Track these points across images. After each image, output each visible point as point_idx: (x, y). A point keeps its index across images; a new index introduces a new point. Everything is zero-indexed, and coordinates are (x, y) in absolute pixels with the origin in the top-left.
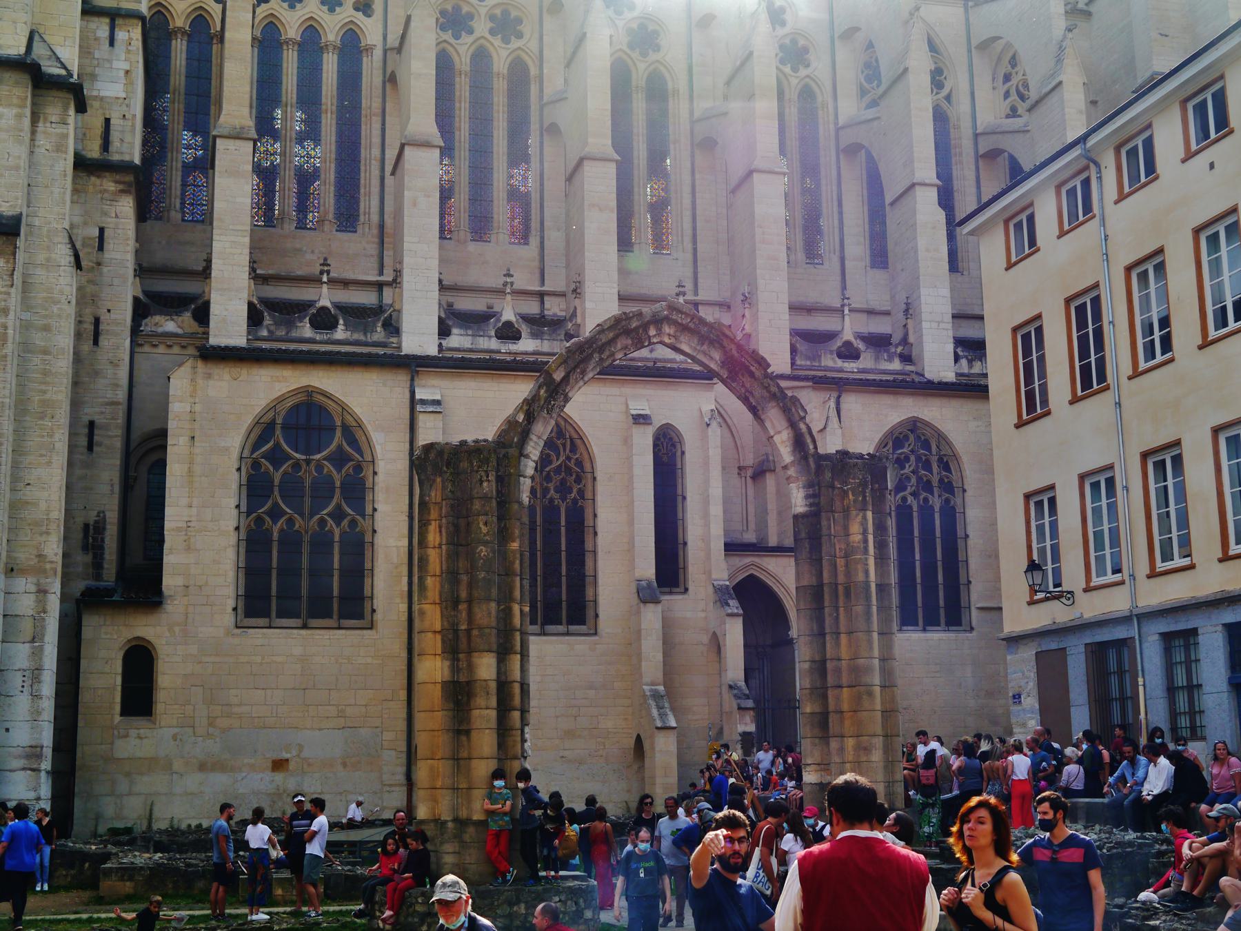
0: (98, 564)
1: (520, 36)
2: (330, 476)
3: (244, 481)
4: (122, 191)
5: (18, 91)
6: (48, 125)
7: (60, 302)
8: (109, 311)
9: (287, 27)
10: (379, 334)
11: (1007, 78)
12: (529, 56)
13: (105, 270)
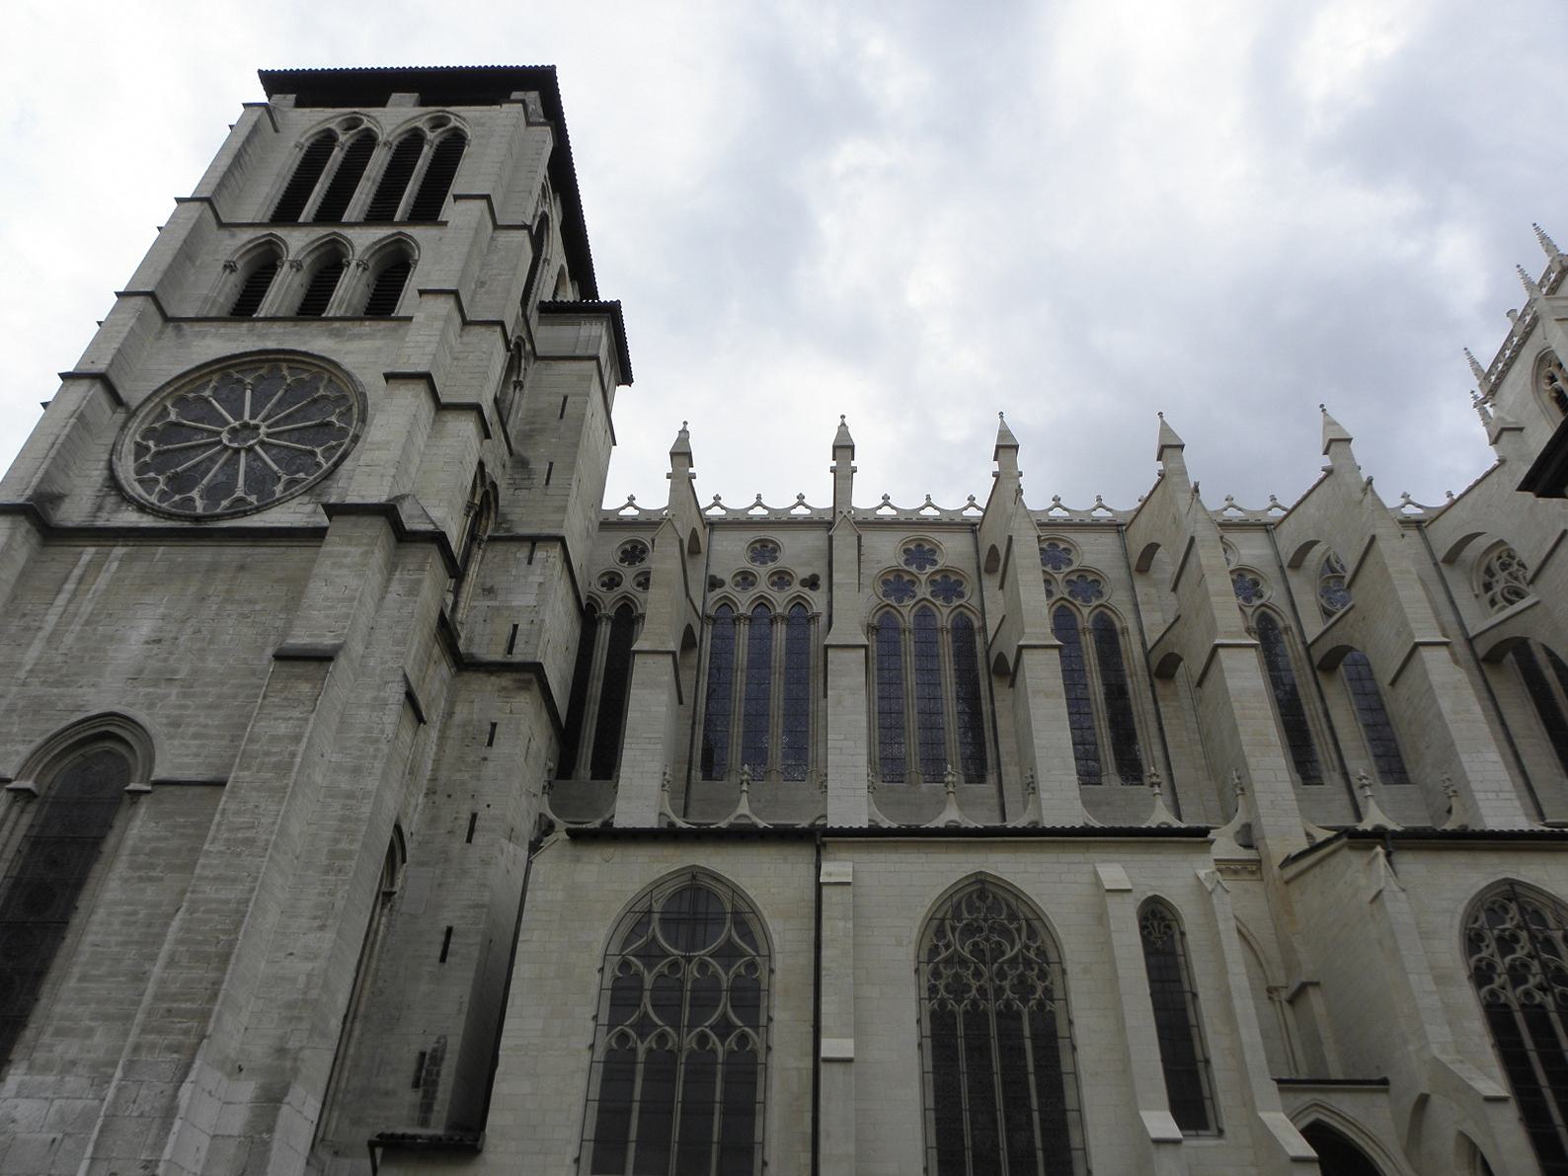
0: (427, 1107)
1: (961, 595)
2: (715, 977)
3: (608, 983)
4: (520, 688)
8: (488, 806)
9: (739, 604)
11: (1488, 587)
12: (973, 612)
13: (491, 764)
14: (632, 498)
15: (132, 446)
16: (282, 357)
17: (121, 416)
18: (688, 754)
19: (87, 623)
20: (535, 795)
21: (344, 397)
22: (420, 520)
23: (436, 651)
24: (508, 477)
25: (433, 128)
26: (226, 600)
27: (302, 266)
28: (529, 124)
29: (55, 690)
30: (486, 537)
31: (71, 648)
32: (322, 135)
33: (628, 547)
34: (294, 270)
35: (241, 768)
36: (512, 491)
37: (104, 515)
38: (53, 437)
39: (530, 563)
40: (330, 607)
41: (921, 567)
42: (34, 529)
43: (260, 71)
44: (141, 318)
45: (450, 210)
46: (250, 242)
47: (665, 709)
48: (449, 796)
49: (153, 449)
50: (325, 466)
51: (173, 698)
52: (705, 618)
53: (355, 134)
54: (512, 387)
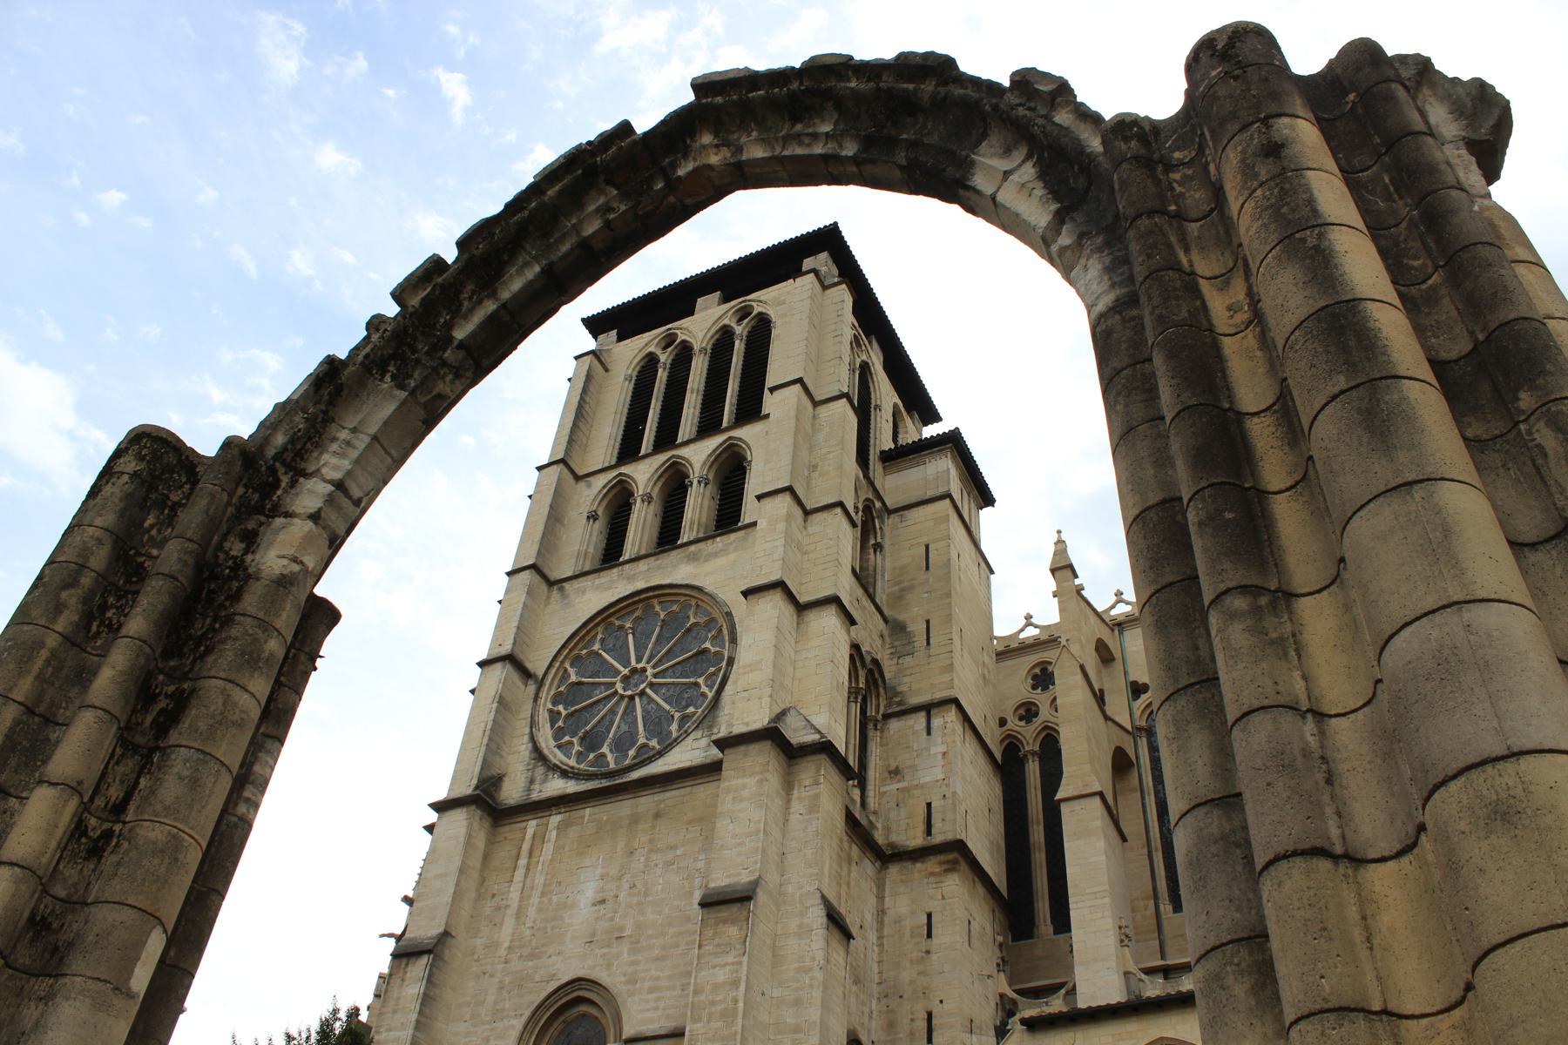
4: (946, 871)
5: (761, 759)
6: (802, 790)
7: (811, 969)
8: (941, 1002)
13: (934, 957)
14: (1028, 617)
15: (547, 715)
16: (651, 594)
17: (532, 688)
18: (1151, 888)
19: (543, 894)
20: (989, 976)
21: (713, 620)
22: (805, 732)
23: (855, 851)
24: (888, 646)
25: (740, 321)
26: (651, 851)
28: (825, 288)
29: (530, 963)
30: (879, 717)
31: (534, 922)
32: (646, 359)
33: (1037, 671)
34: (646, 503)
35: (694, 1021)
36: (896, 660)
37: (536, 787)
38: (483, 724)
39: (929, 733)
40: (740, 844)
42: (486, 816)
43: (583, 320)
44: (530, 592)
45: (770, 403)
46: (604, 487)
47: (1104, 858)
48: (901, 997)
49: (564, 713)
50: (710, 695)
51: (625, 955)
52: (1136, 732)
53: (673, 350)
54: (872, 551)
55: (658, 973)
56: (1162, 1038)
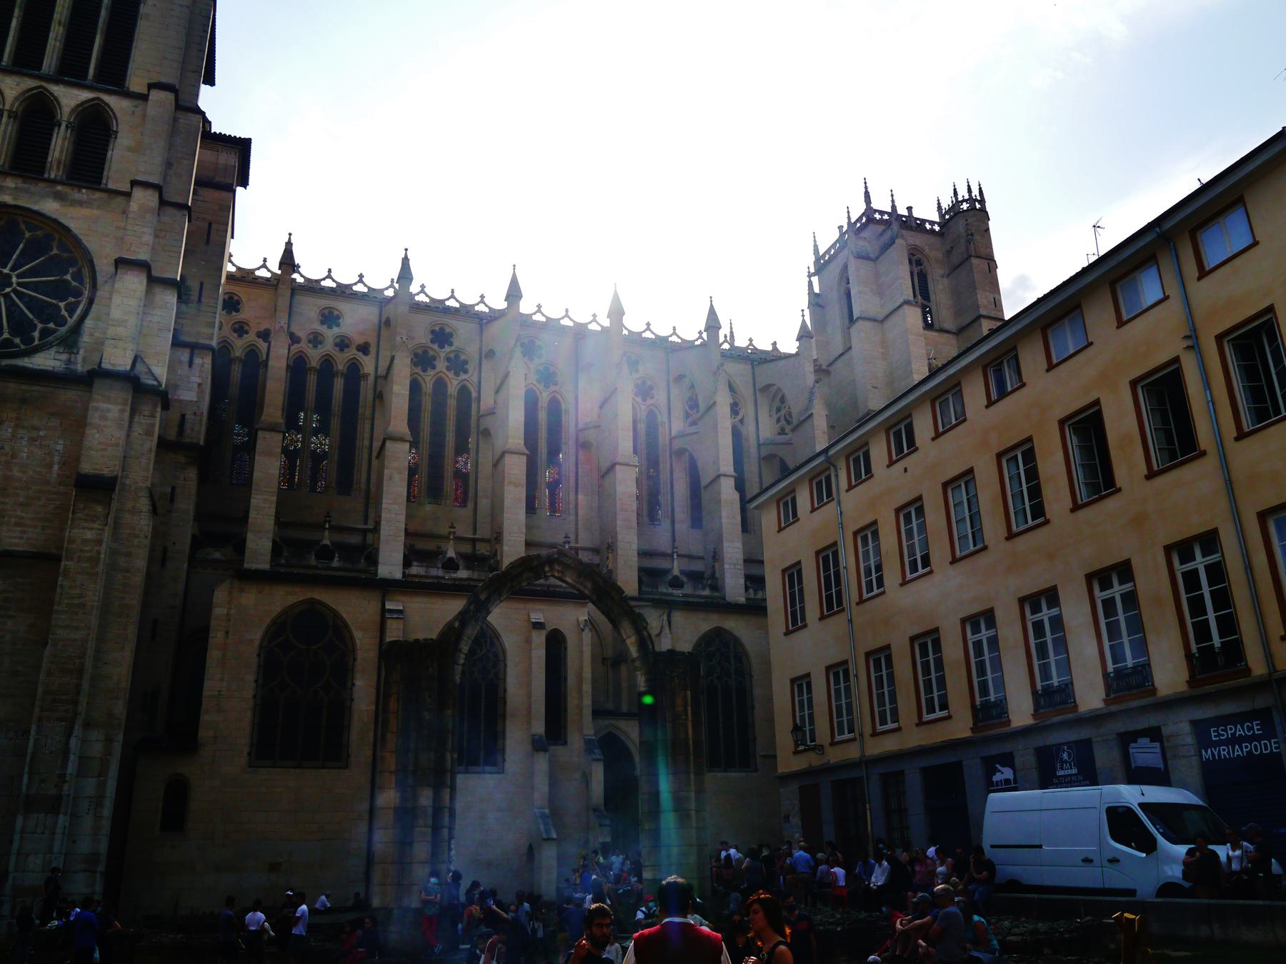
1: (466, 372)
6: (142, 417)
7: (138, 536)
8: (174, 543)
10: (362, 564)
11: (778, 410)
12: (472, 385)
22: (146, 377)
27: (17, 115)
40: (103, 450)
41: (442, 347)
55: (24, 515)
56: (312, 598)
